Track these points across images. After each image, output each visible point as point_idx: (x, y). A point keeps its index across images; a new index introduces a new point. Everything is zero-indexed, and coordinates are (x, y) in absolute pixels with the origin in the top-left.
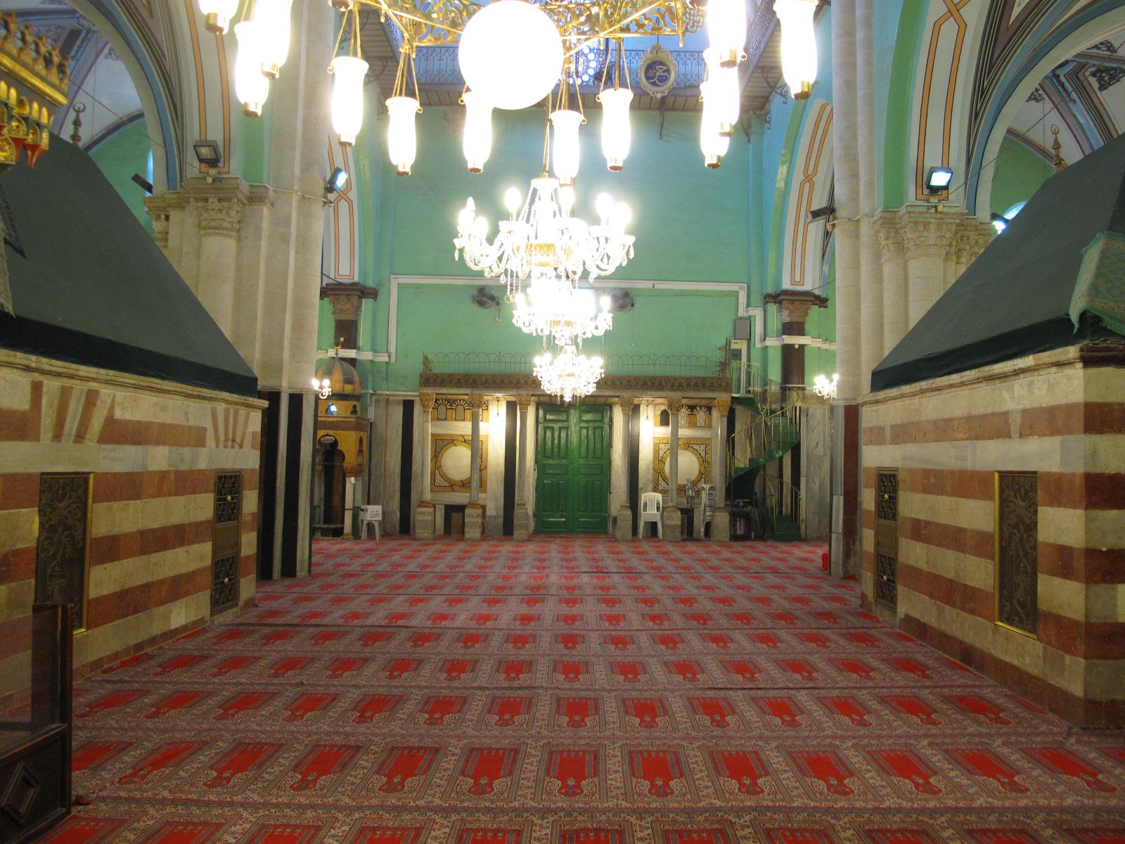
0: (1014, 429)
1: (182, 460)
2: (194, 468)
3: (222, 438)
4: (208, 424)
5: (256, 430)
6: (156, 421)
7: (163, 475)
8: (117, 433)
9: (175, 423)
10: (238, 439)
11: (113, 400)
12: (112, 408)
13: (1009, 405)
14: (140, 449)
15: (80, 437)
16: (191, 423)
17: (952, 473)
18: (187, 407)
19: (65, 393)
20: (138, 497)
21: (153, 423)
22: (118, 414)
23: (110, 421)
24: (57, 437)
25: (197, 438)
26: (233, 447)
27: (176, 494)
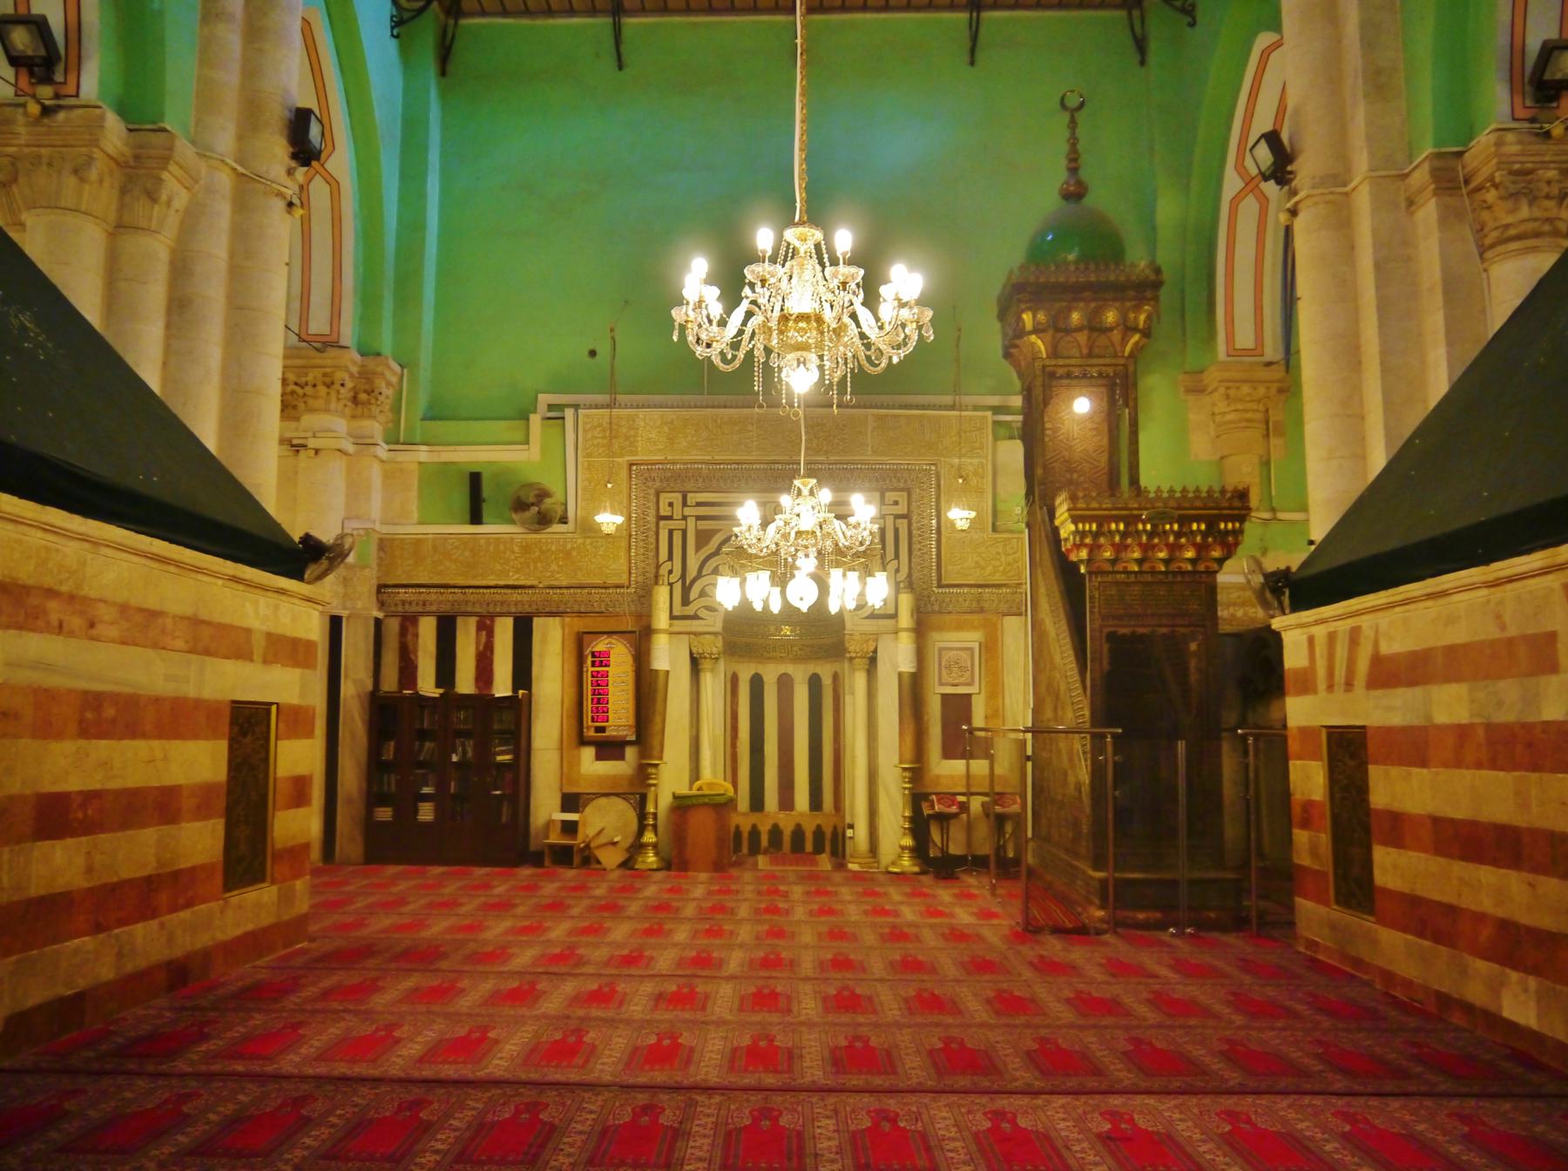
0: (258, 652)
1: (1500, 704)
2: (1531, 719)
6: (1439, 644)
7: (1462, 732)
9: (1476, 638)
11: (1377, 632)
13: (253, 622)
14: (1417, 692)
15: (1349, 685)
16: (1512, 631)
17: (157, 701)
18: (1501, 602)
19: (1332, 637)
20: (1423, 763)
21: (1432, 649)
22: (1386, 649)
23: (1377, 660)
24: (1330, 687)
27: (1494, 765)
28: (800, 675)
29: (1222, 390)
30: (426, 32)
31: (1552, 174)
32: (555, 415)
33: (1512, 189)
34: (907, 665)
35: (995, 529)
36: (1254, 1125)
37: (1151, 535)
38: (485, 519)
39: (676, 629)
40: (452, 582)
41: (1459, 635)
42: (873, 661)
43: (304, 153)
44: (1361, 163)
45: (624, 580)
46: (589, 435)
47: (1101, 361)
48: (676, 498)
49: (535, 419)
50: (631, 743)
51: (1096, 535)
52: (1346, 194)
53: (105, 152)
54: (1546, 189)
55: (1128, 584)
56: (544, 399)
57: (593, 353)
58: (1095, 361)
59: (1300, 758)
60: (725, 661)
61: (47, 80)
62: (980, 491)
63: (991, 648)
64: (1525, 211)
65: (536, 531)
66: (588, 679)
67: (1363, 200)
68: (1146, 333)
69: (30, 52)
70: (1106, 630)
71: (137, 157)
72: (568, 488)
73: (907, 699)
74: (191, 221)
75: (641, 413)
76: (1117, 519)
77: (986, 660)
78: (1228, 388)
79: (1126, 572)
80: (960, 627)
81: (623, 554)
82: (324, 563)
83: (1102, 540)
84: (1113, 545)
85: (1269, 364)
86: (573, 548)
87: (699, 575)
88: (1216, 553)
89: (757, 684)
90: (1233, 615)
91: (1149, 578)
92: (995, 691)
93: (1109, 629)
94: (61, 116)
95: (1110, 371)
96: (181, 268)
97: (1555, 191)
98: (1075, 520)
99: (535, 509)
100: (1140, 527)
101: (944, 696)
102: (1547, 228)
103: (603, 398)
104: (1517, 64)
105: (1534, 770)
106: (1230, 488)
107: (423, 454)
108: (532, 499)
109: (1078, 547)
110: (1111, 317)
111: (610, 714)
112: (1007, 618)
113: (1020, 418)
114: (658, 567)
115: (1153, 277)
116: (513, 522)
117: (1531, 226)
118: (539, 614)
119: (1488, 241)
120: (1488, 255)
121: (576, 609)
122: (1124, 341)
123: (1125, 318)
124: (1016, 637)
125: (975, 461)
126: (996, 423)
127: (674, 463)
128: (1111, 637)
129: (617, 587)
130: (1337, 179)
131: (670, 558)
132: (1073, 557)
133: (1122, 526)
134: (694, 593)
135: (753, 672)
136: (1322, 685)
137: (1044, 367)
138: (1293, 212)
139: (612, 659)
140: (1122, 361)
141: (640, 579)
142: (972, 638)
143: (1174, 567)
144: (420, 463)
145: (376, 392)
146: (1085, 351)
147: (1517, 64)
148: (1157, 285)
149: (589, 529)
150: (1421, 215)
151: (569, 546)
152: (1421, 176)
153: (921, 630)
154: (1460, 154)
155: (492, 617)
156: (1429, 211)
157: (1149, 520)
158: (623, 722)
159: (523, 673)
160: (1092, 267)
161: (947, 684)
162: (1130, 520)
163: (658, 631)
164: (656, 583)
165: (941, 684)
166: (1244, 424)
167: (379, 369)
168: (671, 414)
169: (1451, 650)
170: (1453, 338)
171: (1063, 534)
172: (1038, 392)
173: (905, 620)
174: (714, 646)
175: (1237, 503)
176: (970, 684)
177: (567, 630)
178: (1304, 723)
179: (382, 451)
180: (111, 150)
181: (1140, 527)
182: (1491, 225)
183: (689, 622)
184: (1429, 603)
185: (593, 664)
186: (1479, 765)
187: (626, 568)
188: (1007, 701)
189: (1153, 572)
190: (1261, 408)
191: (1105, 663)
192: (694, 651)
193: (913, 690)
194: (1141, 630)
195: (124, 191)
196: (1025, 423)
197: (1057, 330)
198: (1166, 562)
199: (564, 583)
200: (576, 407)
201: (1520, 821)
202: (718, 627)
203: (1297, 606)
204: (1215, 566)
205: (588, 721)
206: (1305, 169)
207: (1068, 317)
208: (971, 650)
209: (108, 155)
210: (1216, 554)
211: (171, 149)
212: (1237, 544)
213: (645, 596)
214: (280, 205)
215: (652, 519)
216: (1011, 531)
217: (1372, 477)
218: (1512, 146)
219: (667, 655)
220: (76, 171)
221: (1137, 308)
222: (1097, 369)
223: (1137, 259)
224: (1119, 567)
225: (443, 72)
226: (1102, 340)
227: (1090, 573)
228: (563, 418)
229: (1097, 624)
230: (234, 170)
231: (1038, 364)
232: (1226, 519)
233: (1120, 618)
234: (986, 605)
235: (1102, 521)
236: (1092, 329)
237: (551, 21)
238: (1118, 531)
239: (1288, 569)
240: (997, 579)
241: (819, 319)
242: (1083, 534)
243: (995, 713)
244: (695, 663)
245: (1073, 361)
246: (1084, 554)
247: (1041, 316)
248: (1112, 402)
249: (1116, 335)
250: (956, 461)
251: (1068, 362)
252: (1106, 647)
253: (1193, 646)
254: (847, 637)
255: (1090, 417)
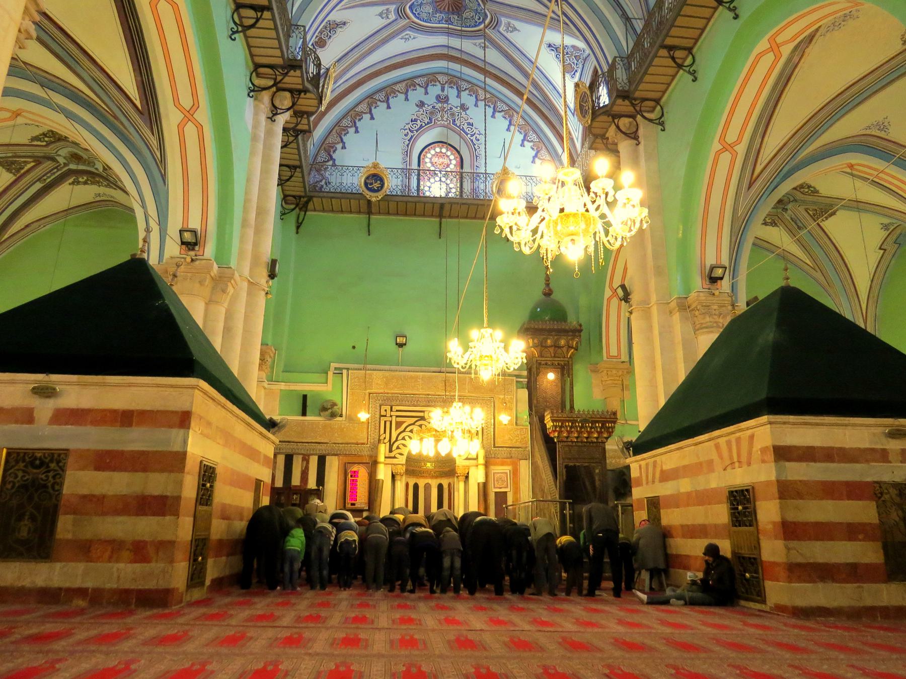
2: (707, 488)
3: (728, 462)
4: (714, 456)
5: (764, 445)
7: (689, 494)
8: (666, 476)
10: (744, 459)
12: (662, 466)
13: (261, 450)
15: (653, 482)
16: (701, 459)
19: (647, 465)
22: (665, 468)
23: (662, 472)
24: (647, 483)
25: (710, 465)
26: (739, 467)
28: (434, 483)
29: (605, 372)
30: (292, 218)
31: (715, 307)
32: (339, 372)
33: (703, 311)
34: (482, 479)
35: (516, 425)
36: (622, 670)
37: (581, 428)
38: (307, 414)
39: (386, 462)
40: (292, 440)
41: (686, 462)
42: (467, 477)
43: (272, 276)
44: (654, 298)
45: (365, 441)
46: (353, 381)
47: (559, 359)
48: (388, 408)
49: (330, 374)
50: (366, 510)
51: (561, 427)
52: (649, 308)
53: (211, 275)
54: (714, 312)
55: (572, 446)
56: (333, 365)
57: (354, 347)
58: (556, 359)
59: (637, 510)
60: (406, 477)
61: (193, 249)
62: (511, 409)
63: (515, 473)
64: (708, 319)
65: (330, 420)
66: (349, 483)
67: (655, 311)
68: (576, 349)
69: (189, 241)
70: (564, 464)
71: (220, 277)
72: (344, 404)
73: (482, 494)
74: (234, 300)
75: (375, 372)
76: (568, 421)
77: (513, 478)
78: (607, 371)
79: (572, 442)
80: (503, 464)
81: (365, 431)
82: (276, 428)
83: (563, 429)
84: (567, 431)
85: (623, 362)
86: (344, 428)
87: (397, 440)
88: (605, 435)
89: (416, 487)
90: (611, 462)
91: (580, 444)
92: (517, 490)
93: (566, 464)
94: (197, 263)
95: (562, 363)
96: (229, 316)
97: (717, 312)
98: (553, 421)
99: (330, 411)
100: (577, 424)
101: (496, 493)
102: (715, 325)
103: (361, 366)
104: (703, 272)
105: (709, 505)
106: (610, 411)
107: (282, 386)
108: (329, 407)
109: (554, 431)
110: (562, 342)
111: (358, 498)
112: (522, 462)
113: (526, 380)
114: (380, 436)
115: (578, 328)
116: (320, 415)
117: (709, 324)
118: (329, 455)
119: (696, 328)
120: (697, 332)
121: (344, 453)
122: (568, 352)
123: (568, 342)
124: (525, 468)
125: (509, 397)
126: (517, 381)
127: (388, 394)
128: (566, 467)
129: (362, 444)
130: (646, 302)
131: (385, 432)
132: (552, 436)
133: (570, 424)
134: (394, 447)
135: (414, 482)
136: (644, 482)
137: (537, 361)
138: (631, 313)
139: (359, 475)
140: (566, 359)
141: (372, 441)
142: (507, 469)
143: (589, 440)
144: (281, 390)
145: (266, 360)
146: (553, 355)
147: (703, 272)
148: (580, 331)
149: (352, 419)
150: (674, 317)
151: (343, 426)
152: (673, 304)
153: (487, 465)
154: (687, 298)
155: (309, 455)
156: (677, 317)
157: (581, 421)
158: (363, 501)
159: (321, 480)
160: (555, 323)
161: (497, 488)
162: (573, 422)
163: (380, 463)
164: (379, 443)
165: (494, 488)
166: (614, 385)
167: (268, 351)
168: (387, 374)
169: (685, 467)
170: (686, 361)
171: (548, 426)
172: (534, 370)
173: (481, 460)
174: (402, 469)
175: (612, 416)
176: (507, 487)
177: (340, 461)
178: (638, 497)
179: (265, 384)
180: (212, 275)
181: (577, 424)
182: (697, 323)
183: (391, 459)
184: (678, 451)
185: (351, 476)
186: (694, 505)
187: (366, 436)
188: (521, 495)
189: (582, 442)
190: (620, 379)
191: (564, 477)
192: (394, 472)
193: (484, 489)
194: (578, 464)
195: (213, 288)
196: (528, 382)
197: (542, 346)
198: (587, 438)
199: (340, 442)
200: (348, 369)
201: (706, 522)
202: (404, 462)
203: (635, 454)
204: (605, 440)
205: (348, 500)
206: (635, 298)
207: (546, 341)
208: (506, 473)
209: (212, 277)
210: (605, 435)
211: (233, 274)
212: (613, 432)
213: (375, 448)
214: (263, 293)
215: (378, 416)
216: (523, 426)
217: (660, 408)
218: (702, 297)
219: (383, 473)
220: (200, 282)
221: (573, 339)
222: (556, 362)
223: (572, 321)
224: (569, 440)
225: (297, 233)
226: (559, 351)
227: (558, 441)
228: (342, 374)
229: (561, 462)
230: (249, 281)
231: (534, 360)
232: (609, 422)
233: (570, 459)
234: (513, 455)
235: (563, 422)
236: (555, 347)
237: (342, 215)
238: (569, 426)
239: (632, 441)
240: (518, 445)
241: (491, 357)
242: (556, 427)
243: (516, 499)
244: (393, 476)
245: (548, 359)
246: (556, 434)
247: (536, 341)
248: (563, 375)
249: (565, 349)
250: (502, 397)
251: (546, 359)
252: (564, 471)
253: (597, 471)
254: (457, 467)
255: (553, 381)
